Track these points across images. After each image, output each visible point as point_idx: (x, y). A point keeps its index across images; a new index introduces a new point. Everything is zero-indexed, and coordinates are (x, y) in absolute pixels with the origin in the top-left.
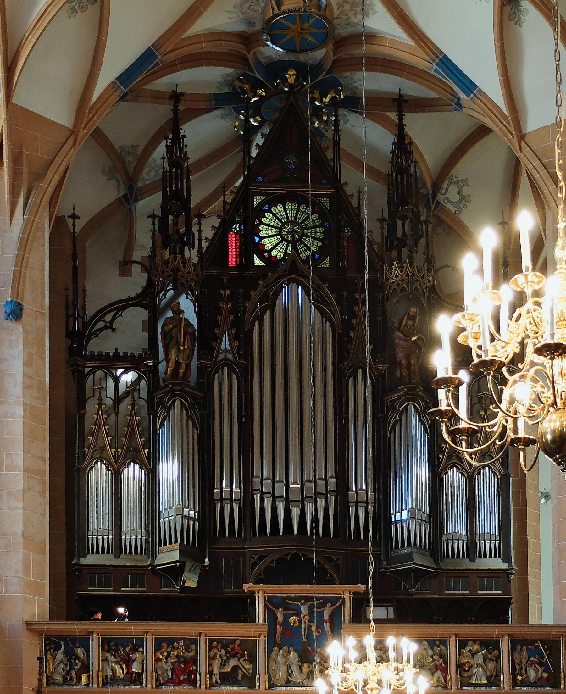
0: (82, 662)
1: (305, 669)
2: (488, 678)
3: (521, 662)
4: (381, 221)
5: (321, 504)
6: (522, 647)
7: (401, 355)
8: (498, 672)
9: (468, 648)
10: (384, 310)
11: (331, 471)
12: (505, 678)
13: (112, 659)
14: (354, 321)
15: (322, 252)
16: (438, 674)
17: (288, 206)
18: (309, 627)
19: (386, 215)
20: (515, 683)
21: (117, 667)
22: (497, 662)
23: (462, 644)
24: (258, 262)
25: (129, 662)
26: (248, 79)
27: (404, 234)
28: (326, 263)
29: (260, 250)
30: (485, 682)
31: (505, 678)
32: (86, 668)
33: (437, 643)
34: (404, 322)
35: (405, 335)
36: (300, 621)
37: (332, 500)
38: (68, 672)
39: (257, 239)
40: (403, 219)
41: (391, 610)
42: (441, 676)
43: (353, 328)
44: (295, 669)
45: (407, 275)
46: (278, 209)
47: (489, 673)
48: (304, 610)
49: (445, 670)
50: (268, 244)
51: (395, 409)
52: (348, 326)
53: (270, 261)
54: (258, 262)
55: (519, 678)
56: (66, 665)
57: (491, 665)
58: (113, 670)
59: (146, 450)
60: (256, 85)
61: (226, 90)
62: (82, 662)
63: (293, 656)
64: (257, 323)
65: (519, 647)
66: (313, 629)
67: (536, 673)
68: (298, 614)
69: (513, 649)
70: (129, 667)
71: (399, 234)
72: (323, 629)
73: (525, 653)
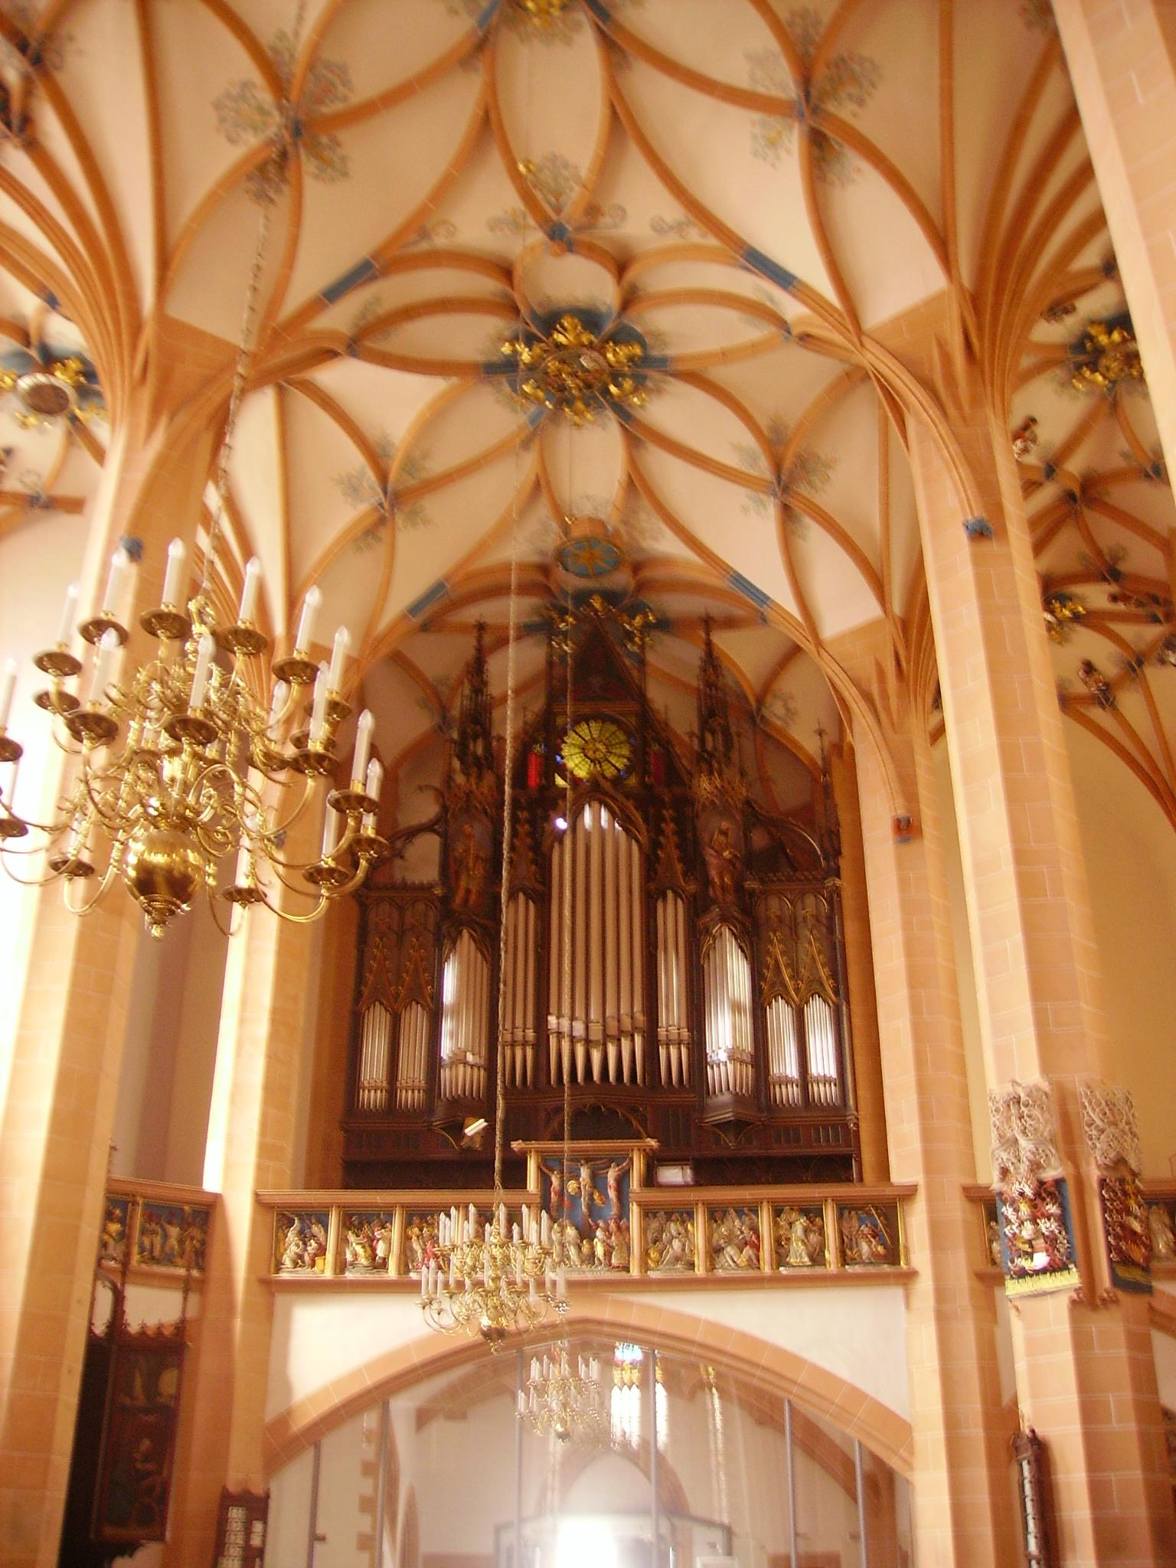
0: (320, 1244)
1: (586, 1247)
2: (811, 1258)
3: (850, 1232)
4: (691, 735)
5: (625, 1044)
6: (850, 1213)
7: (713, 873)
8: (822, 1247)
9: (783, 1216)
10: (695, 828)
11: (638, 1007)
12: (831, 1255)
13: (351, 1237)
14: (662, 839)
15: (629, 770)
16: (748, 1251)
17: (593, 724)
18: (591, 1198)
19: (696, 731)
20: (844, 1259)
21: (359, 1250)
22: (820, 1234)
23: (777, 1212)
24: (560, 781)
25: (371, 1245)
26: (555, 607)
27: (715, 748)
28: (632, 781)
29: (562, 770)
30: (806, 1259)
31: (831, 1255)
32: (322, 1250)
33: (746, 1209)
34: (715, 837)
35: (716, 851)
36: (579, 1188)
37: (638, 1039)
38: (301, 1257)
39: (558, 758)
40: (713, 733)
41: (689, 1171)
42: (751, 1252)
43: (659, 845)
44: (572, 1251)
45: (716, 787)
46: (583, 729)
47: (811, 1250)
48: (584, 1173)
49: (757, 1247)
50: (570, 764)
51: (708, 932)
52: (656, 845)
53: (576, 782)
54: (560, 781)
55: (849, 1252)
56: (297, 1245)
57: (814, 1238)
58: (355, 1255)
59: (429, 987)
60: (563, 612)
61: (536, 619)
62: (320, 1244)
63: (571, 1232)
64: (556, 845)
65: (846, 1213)
66: (596, 1196)
67: (870, 1246)
68: (577, 1177)
69: (840, 1217)
70: (374, 1250)
71: (709, 746)
72: (607, 1196)
73: (855, 1222)
